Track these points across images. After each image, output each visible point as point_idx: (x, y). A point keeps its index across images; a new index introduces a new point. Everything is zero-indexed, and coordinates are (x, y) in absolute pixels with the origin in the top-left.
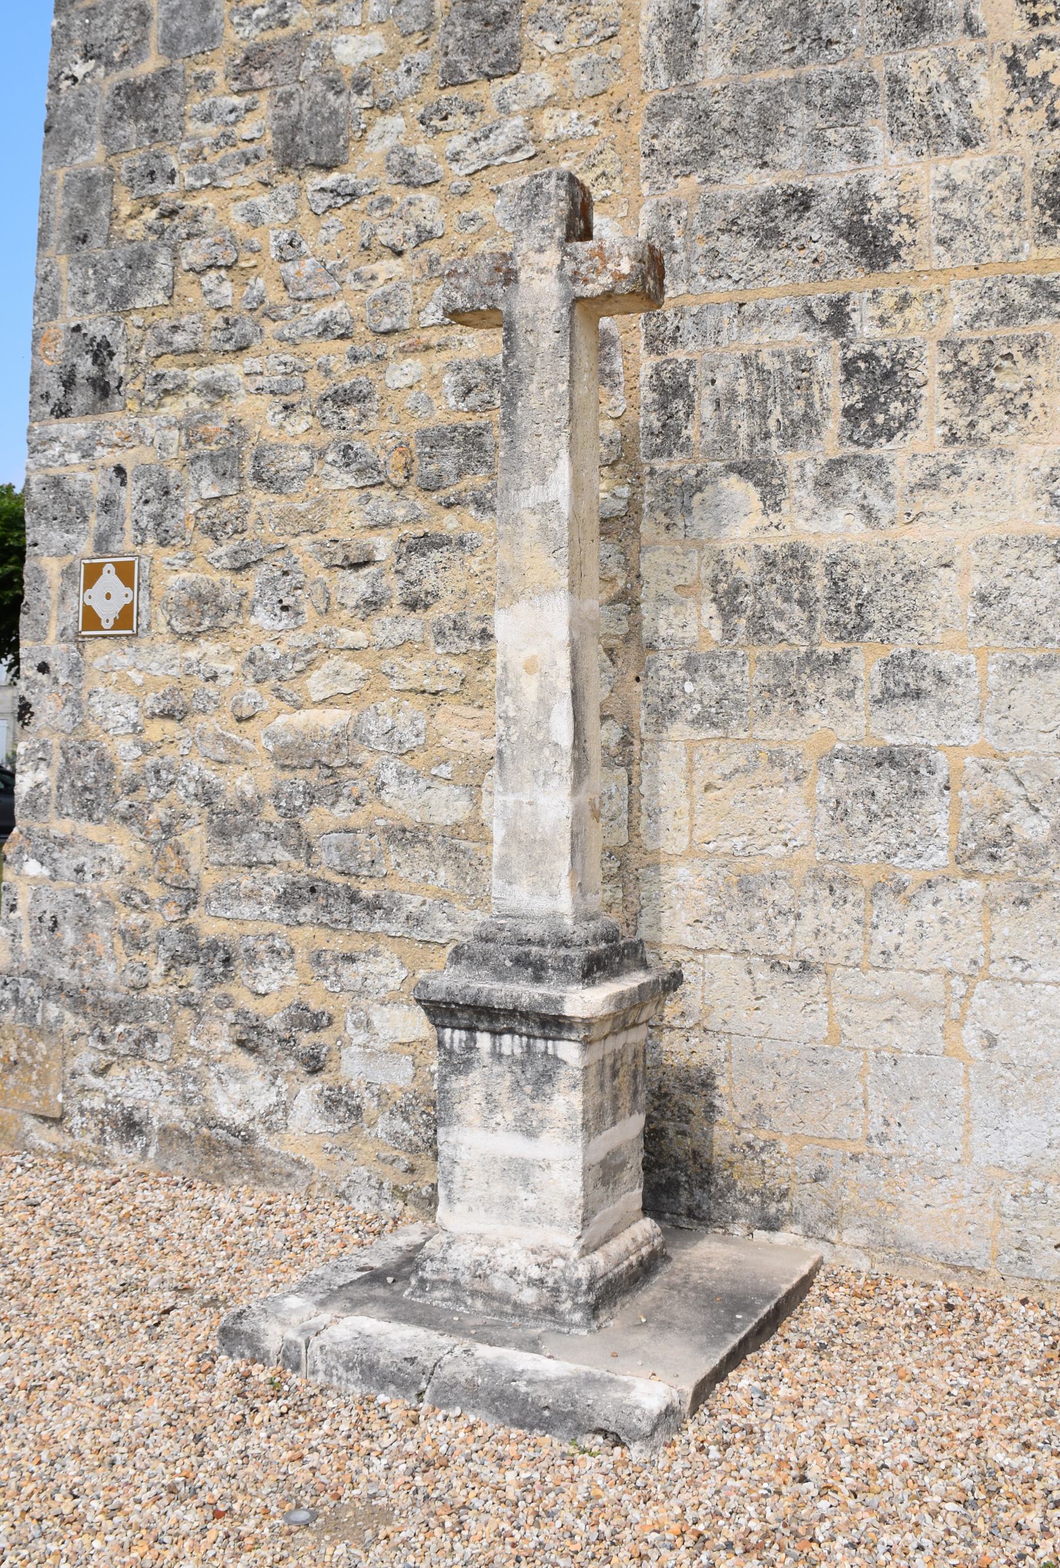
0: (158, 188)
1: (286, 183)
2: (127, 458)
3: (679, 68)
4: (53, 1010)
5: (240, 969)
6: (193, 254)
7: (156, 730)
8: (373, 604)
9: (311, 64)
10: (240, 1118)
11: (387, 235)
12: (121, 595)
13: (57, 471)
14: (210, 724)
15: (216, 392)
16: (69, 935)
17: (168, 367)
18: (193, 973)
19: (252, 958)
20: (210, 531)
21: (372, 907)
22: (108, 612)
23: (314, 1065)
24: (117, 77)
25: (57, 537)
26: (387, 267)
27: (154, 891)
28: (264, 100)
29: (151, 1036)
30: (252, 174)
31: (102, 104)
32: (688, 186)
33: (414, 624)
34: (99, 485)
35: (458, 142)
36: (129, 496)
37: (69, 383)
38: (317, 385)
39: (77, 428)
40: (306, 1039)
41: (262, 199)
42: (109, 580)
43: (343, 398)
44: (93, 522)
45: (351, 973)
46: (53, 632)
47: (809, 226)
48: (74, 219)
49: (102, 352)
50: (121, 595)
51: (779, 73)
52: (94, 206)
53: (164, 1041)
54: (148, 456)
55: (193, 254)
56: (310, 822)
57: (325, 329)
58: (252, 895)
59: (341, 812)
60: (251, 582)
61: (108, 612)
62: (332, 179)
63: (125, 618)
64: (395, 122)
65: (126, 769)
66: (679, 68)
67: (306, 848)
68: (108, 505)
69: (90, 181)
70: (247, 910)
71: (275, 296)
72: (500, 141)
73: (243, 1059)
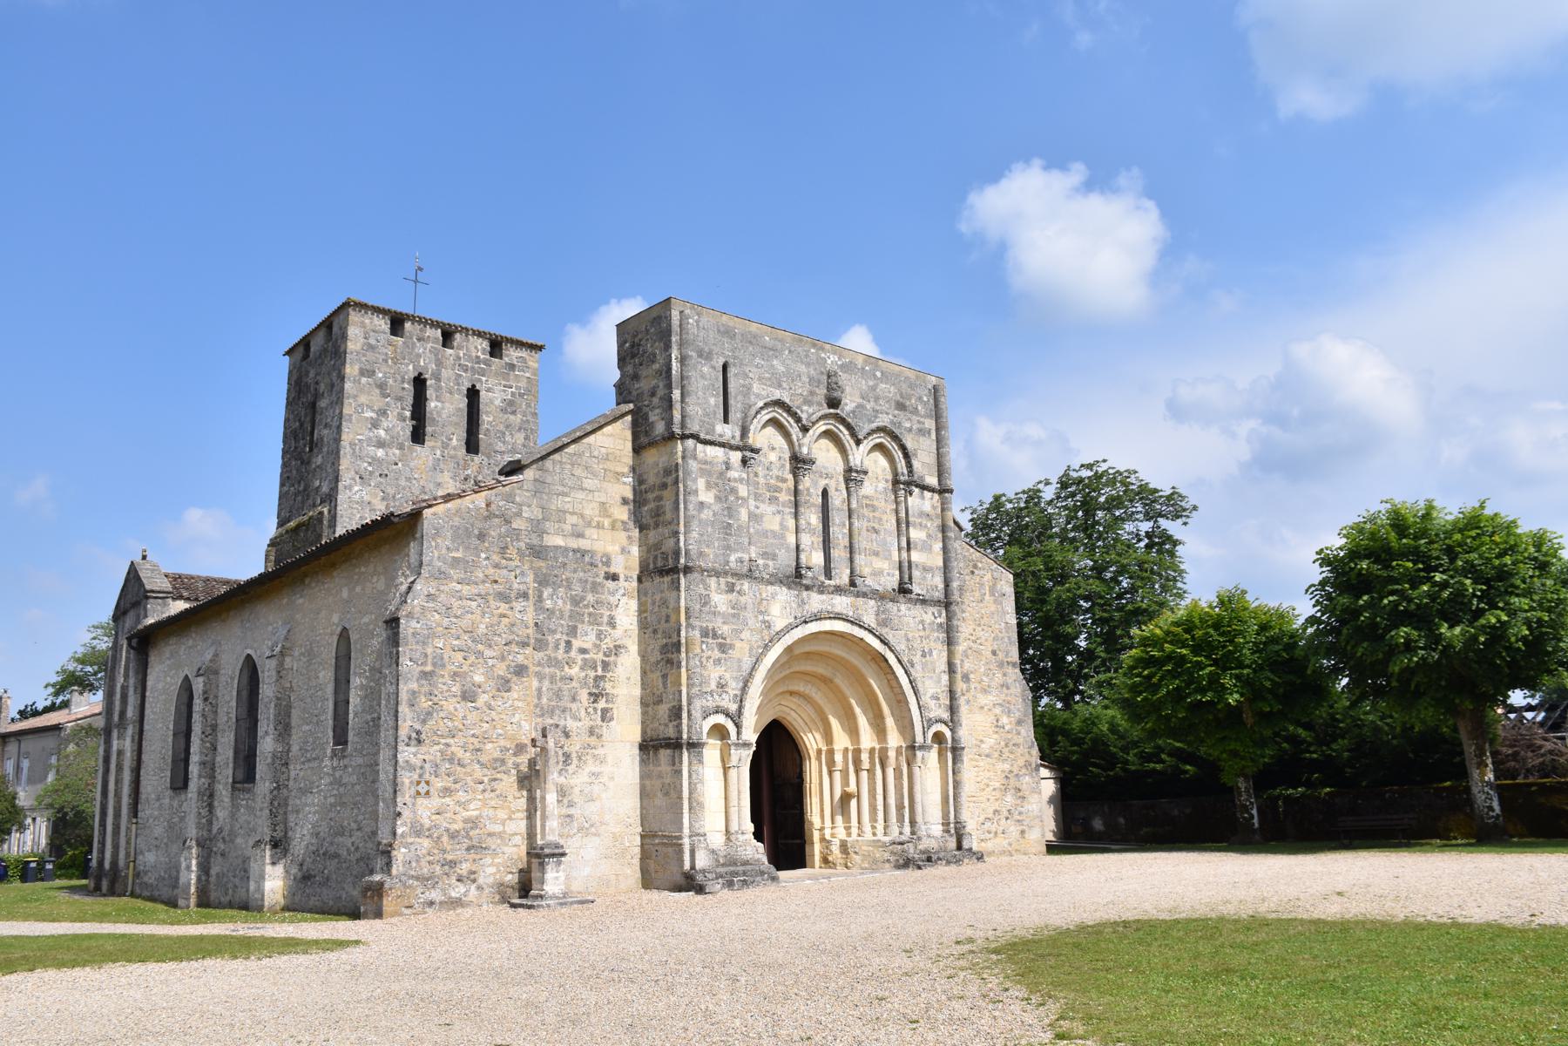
0: (432, 697)
1: (463, 703)
2: (426, 757)
3: (539, 699)
4: (411, 882)
5: (458, 865)
6: (442, 714)
7: (434, 817)
8: (484, 791)
9: (469, 679)
10: (458, 895)
11: (486, 719)
12: (426, 788)
13: (407, 758)
14: (448, 815)
15: (447, 745)
16: (414, 864)
17: (435, 738)
18: (447, 867)
19: (461, 862)
20: (448, 775)
21: (485, 848)
22: (423, 791)
23: (474, 881)
24: (420, 668)
25: (408, 774)
26: (485, 725)
27: (436, 851)
28: (458, 684)
29: (437, 883)
30: (455, 700)
31: (416, 674)
32: (539, 720)
33: (492, 795)
34: (419, 764)
35: (500, 703)
36: (427, 766)
37: (410, 738)
38: (471, 747)
39: (413, 749)
40: (472, 877)
41: (458, 706)
42: (423, 784)
43: (478, 750)
44: (418, 771)
45: (481, 862)
46: (407, 796)
47: (558, 730)
48: (409, 700)
49: (418, 733)
50: (426, 788)
52: (415, 698)
53: (440, 883)
54: (432, 758)
55: (442, 714)
56: (471, 833)
57: (473, 735)
59: (477, 831)
60: (458, 786)
61: (423, 791)
62: (473, 705)
63: (428, 793)
64: (486, 695)
65: (427, 826)
66: (539, 699)
67: (471, 839)
68: (422, 768)
69: (414, 692)
70: (458, 853)
71: (461, 727)
72: (507, 705)
73: (459, 883)
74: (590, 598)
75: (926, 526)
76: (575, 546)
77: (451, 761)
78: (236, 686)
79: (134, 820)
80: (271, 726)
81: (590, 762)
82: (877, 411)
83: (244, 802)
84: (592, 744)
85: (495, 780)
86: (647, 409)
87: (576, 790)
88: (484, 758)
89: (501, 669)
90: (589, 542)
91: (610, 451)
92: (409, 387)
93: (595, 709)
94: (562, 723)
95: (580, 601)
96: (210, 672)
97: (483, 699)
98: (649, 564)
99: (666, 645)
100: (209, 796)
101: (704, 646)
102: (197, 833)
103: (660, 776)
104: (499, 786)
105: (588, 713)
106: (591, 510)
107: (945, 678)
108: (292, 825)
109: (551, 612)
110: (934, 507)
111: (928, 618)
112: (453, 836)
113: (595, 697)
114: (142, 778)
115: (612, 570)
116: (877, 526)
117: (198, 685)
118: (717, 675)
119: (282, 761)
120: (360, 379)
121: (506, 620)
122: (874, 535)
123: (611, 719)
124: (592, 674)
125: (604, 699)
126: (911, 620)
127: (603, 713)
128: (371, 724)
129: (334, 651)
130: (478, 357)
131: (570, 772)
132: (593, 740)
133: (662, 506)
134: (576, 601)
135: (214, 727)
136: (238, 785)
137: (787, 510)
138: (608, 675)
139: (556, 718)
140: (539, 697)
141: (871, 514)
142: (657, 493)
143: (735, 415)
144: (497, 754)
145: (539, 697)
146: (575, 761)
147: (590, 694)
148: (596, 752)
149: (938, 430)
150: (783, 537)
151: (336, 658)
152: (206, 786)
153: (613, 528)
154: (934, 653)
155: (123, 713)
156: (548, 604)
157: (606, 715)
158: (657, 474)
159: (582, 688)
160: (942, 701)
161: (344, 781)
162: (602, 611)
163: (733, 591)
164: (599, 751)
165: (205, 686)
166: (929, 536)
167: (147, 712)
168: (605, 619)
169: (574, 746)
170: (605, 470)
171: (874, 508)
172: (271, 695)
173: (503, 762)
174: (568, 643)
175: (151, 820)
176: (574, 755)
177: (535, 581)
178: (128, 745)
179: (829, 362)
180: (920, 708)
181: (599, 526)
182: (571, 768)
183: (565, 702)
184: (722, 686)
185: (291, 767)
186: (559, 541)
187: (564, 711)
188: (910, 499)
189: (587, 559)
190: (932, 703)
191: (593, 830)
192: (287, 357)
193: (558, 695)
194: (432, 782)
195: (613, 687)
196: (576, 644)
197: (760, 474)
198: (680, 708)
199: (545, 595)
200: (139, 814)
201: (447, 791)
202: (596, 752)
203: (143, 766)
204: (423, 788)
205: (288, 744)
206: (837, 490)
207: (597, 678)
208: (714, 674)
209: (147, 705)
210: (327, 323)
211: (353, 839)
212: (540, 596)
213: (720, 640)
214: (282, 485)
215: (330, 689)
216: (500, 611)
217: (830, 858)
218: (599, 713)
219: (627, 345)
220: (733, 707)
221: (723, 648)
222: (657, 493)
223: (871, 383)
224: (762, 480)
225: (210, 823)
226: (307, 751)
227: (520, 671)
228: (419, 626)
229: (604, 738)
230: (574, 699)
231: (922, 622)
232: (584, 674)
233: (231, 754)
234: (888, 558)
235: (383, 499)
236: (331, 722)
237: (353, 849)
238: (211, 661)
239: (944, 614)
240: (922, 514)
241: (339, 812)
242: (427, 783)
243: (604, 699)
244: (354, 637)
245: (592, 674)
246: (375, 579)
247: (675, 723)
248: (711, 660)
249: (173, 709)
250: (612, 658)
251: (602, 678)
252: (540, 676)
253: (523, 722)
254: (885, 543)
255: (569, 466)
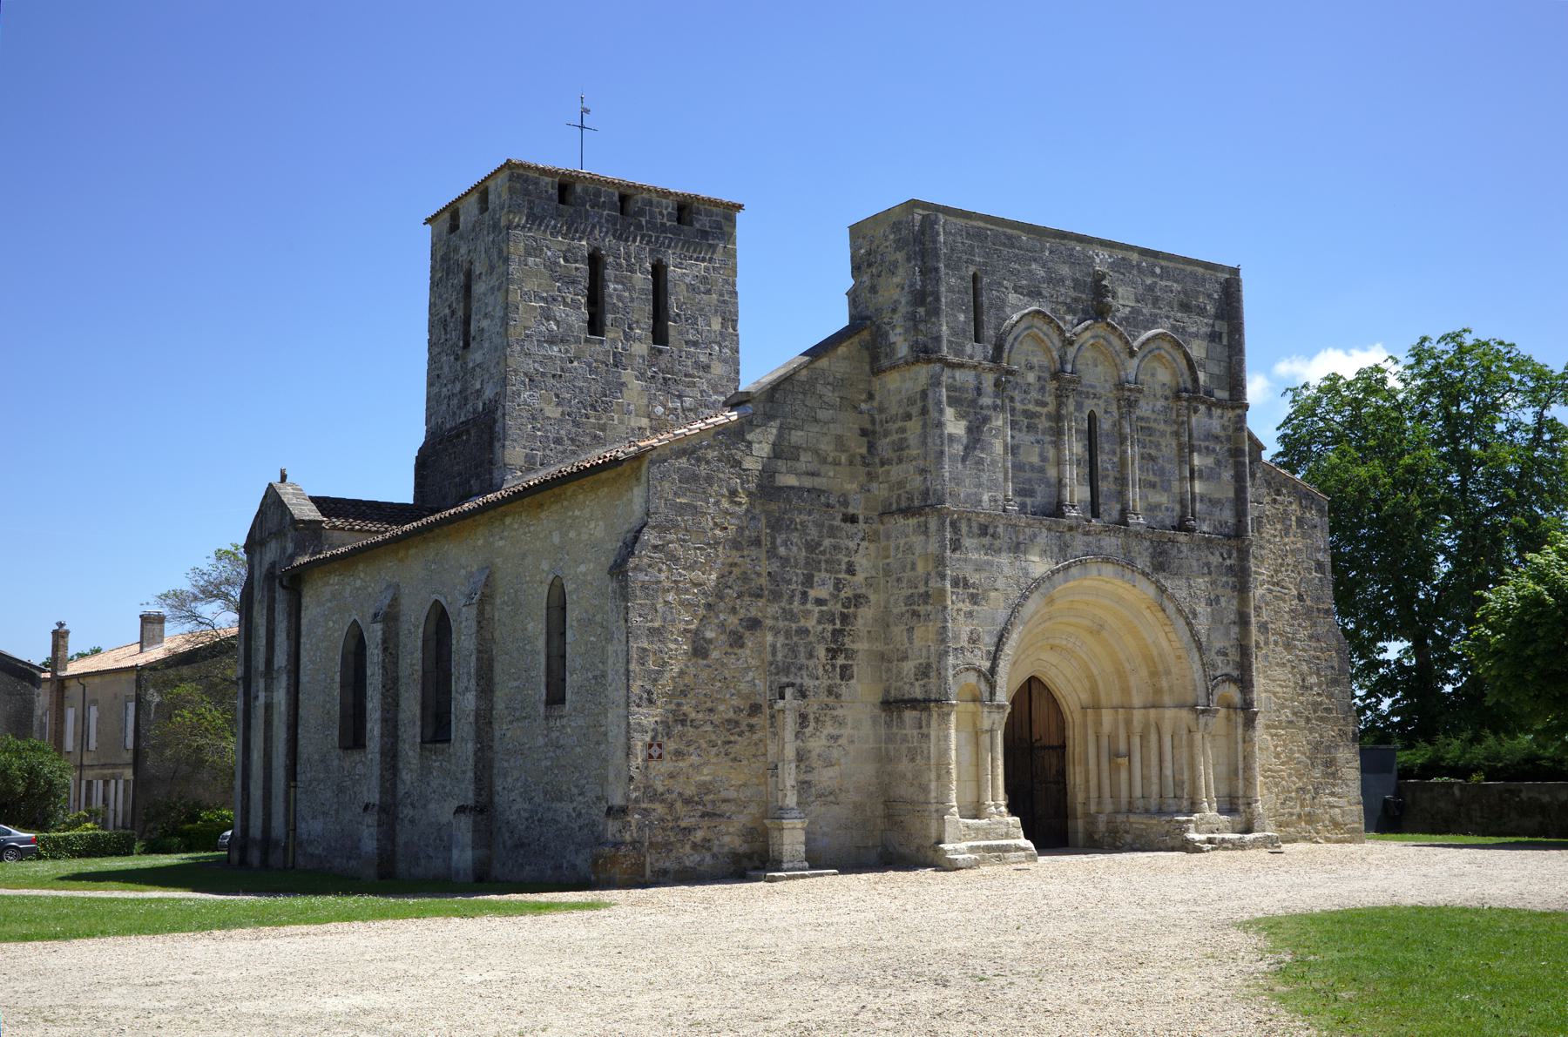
10: (692, 865)
12: (659, 751)
19: (695, 829)
22: (655, 755)
23: (709, 849)
37: (641, 698)
42: (655, 747)
43: (711, 710)
45: (716, 830)
49: (649, 693)
50: (659, 751)
51: (789, 660)
58: (694, 816)
61: (655, 755)
63: (660, 756)
74: (827, 542)
75: (1214, 450)
76: (810, 486)
77: (683, 722)
78: (421, 635)
79: (292, 784)
80: (473, 682)
81: (829, 723)
82: (1156, 315)
83: (438, 764)
84: (831, 704)
85: (730, 742)
86: (888, 328)
87: (814, 754)
88: (716, 718)
89: (733, 621)
90: (824, 480)
91: (846, 376)
92: (584, 267)
93: (833, 666)
94: (798, 681)
95: (816, 548)
96: (390, 617)
97: (715, 654)
98: (891, 504)
99: (912, 595)
100: (391, 756)
101: (954, 597)
102: (381, 798)
103: (904, 740)
104: (734, 749)
105: (826, 671)
106: (826, 446)
107: (1235, 630)
108: (500, 789)
109: (785, 561)
110: (1224, 428)
111: (1215, 560)
112: (687, 802)
113: (833, 653)
114: (300, 736)
115: (851, 511)
116: (1153, 452)
117: (374, 634)
118: (968, 629)
119: (484, 720)
120: (525, 260)
121: (736, 571)
122: (1151, 464)
123: (851, 677)
124: (830, 627)
125: (843, 655)
126: (1194, 563)
127: (841, 670)
128: (593, 681)
129: (545, 600)
130: (663, 225)
131: (808, 735)
132: (831, 700)
133: (906, 439)
134: (812, 547)
135: (396, 680)
136: (427, 746)
137: (1048, 438)
138: (847, 629)
139: (791, 676)
140: (774, 653)
141: (1148, 439)
142: (900, 424)
143: (989, 332)
144: (731, 714)
145: (774, 653)
146: (812, 724)
147: (828, 650)
148: (835, 713)
149: (1230, 334)
150: (1042, 470)
151: (548, 608)
152: (389, 746)
153: (851, 463)
154: (1223, 600)
155: (269, 662)
156: (782, 551)
157: (846, 674)
158: (900, 401)
159: (819, 642)
160: (1231, 658)
161: (562, 742)
162: (840, 556)
163: (986, 534)
164: (839, 712)
165: (384, 634)
166: (1218, 463)
167: (304, 659)
168: (844, 567)
169: (812, 706)
170: (841, 398)
171: (1149, 431)
172: (472, 647)
173: (737, 723)
174: (805, 594)
175: (315, 783)
176: (811, 717)
177: (767, 527)
178: (280, 696)
179: (1098, 260)
180: (1203, 665)
181: (837, 463)
182: (808, 731)
183: (802, 660)
184: (974, 640)
185: (496, 727)
186: (791, 481)
187: (800, 669)
188: (1194, 419)
189: (823, 499)
190: (1219, 660)
191: (831, 798)
192: (428, 226)
193: (793, 650)
194: (664, 746)
195: (853, 642)
196: (812, 593)
197: (1017, 398)
198: (929, 665)
199: (779, 541)
200: (299, 777)
201: (679, 754)
202: (835, 713)
203: (301, 722)
204: (655, 751)
205: (491, 700)
206: (1106, 412)
207: (834, 632)
208: (961, 629)
209: (303, 653)
210: (481, 188)
211: (575, 804)
212: (773, 543)
213: (971, 590)
214: (430, 384)
215: (541, 643)
216: (730, 560)
217: (1096, 837)
218: (838, 669)
219: (863, 251)
220: (986, 665)
221: (974, 599)
222: (900, 424)
223: (1149, 282)
224: (1018, 406)
225: (394, 786)
226: (515, 709)
227: (754, 624)
228: (647, 578)
229: (843, 698)
230: (811, 656)
231: (1208, 565)
232: (820, 628)
233: (417, 710)
234: (1166, 488)
235: (558, 404)
236: (544, 679)
237: (574, 815)
238: (389, 606)
239: (1235, 555)
240: (1210, 436)
241: (556, 775)
242: (660, 746)
243: (843, 655)
244: (569, 587)
245: (830, 627)
246: (592, 525)
247: (922, 682)
248: (962, 613)
249: (338, 658)
250: (852, 610)
251: (841, 631)
252: (776, 632)
253: (757, 681)
254: (1162, 472)
255: (801, 396)
